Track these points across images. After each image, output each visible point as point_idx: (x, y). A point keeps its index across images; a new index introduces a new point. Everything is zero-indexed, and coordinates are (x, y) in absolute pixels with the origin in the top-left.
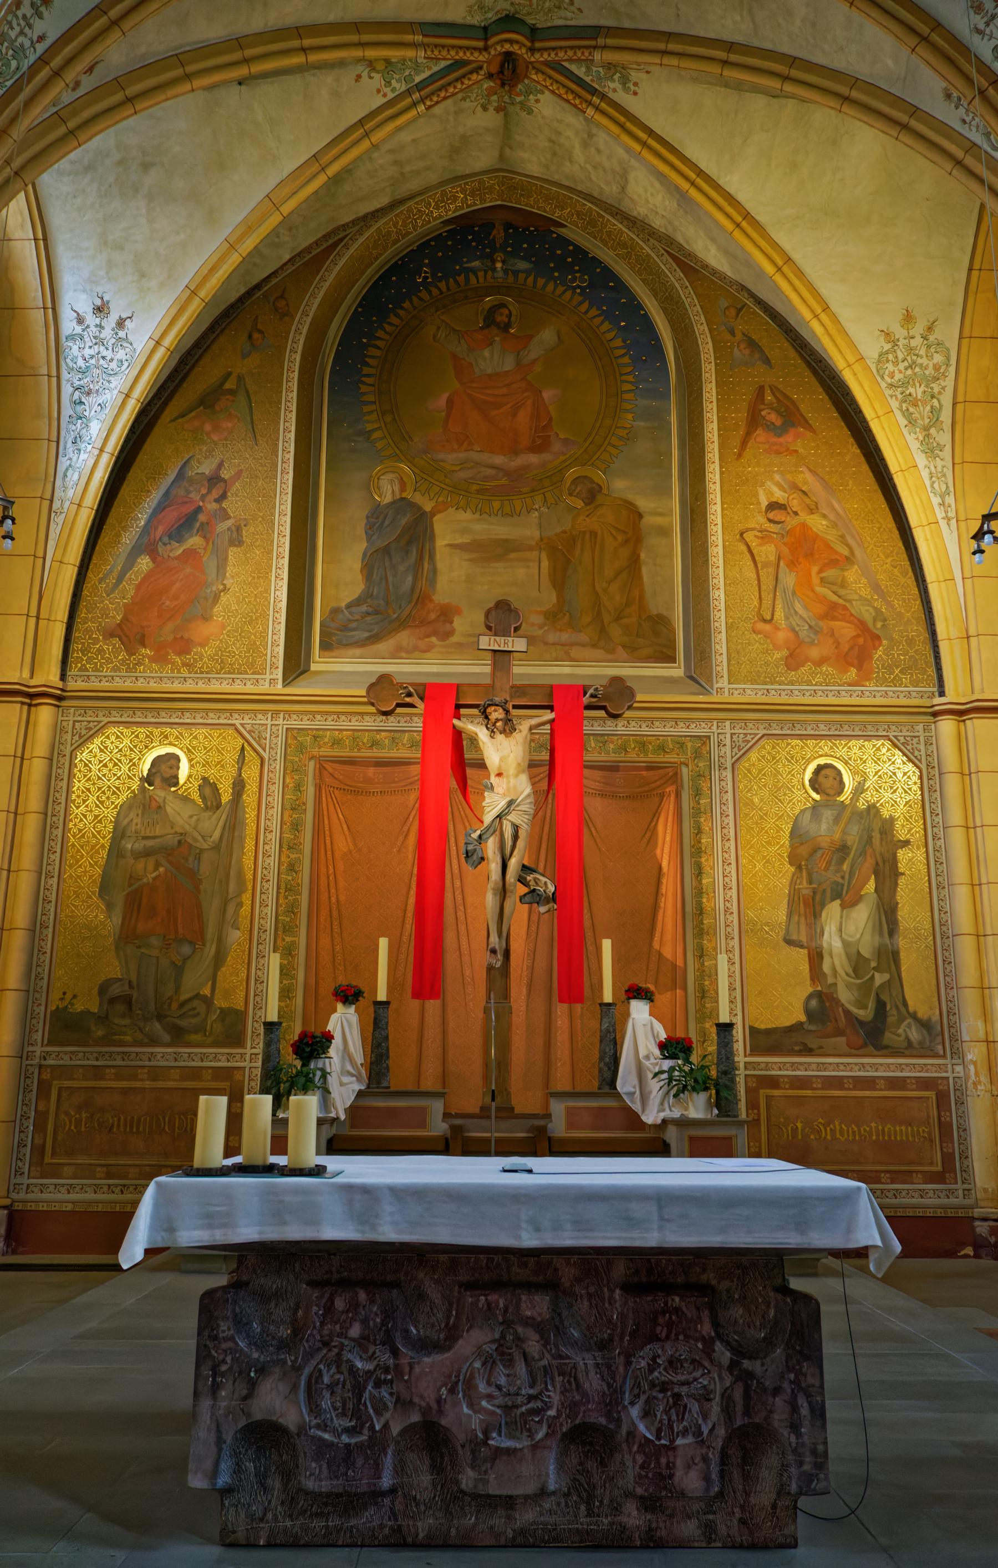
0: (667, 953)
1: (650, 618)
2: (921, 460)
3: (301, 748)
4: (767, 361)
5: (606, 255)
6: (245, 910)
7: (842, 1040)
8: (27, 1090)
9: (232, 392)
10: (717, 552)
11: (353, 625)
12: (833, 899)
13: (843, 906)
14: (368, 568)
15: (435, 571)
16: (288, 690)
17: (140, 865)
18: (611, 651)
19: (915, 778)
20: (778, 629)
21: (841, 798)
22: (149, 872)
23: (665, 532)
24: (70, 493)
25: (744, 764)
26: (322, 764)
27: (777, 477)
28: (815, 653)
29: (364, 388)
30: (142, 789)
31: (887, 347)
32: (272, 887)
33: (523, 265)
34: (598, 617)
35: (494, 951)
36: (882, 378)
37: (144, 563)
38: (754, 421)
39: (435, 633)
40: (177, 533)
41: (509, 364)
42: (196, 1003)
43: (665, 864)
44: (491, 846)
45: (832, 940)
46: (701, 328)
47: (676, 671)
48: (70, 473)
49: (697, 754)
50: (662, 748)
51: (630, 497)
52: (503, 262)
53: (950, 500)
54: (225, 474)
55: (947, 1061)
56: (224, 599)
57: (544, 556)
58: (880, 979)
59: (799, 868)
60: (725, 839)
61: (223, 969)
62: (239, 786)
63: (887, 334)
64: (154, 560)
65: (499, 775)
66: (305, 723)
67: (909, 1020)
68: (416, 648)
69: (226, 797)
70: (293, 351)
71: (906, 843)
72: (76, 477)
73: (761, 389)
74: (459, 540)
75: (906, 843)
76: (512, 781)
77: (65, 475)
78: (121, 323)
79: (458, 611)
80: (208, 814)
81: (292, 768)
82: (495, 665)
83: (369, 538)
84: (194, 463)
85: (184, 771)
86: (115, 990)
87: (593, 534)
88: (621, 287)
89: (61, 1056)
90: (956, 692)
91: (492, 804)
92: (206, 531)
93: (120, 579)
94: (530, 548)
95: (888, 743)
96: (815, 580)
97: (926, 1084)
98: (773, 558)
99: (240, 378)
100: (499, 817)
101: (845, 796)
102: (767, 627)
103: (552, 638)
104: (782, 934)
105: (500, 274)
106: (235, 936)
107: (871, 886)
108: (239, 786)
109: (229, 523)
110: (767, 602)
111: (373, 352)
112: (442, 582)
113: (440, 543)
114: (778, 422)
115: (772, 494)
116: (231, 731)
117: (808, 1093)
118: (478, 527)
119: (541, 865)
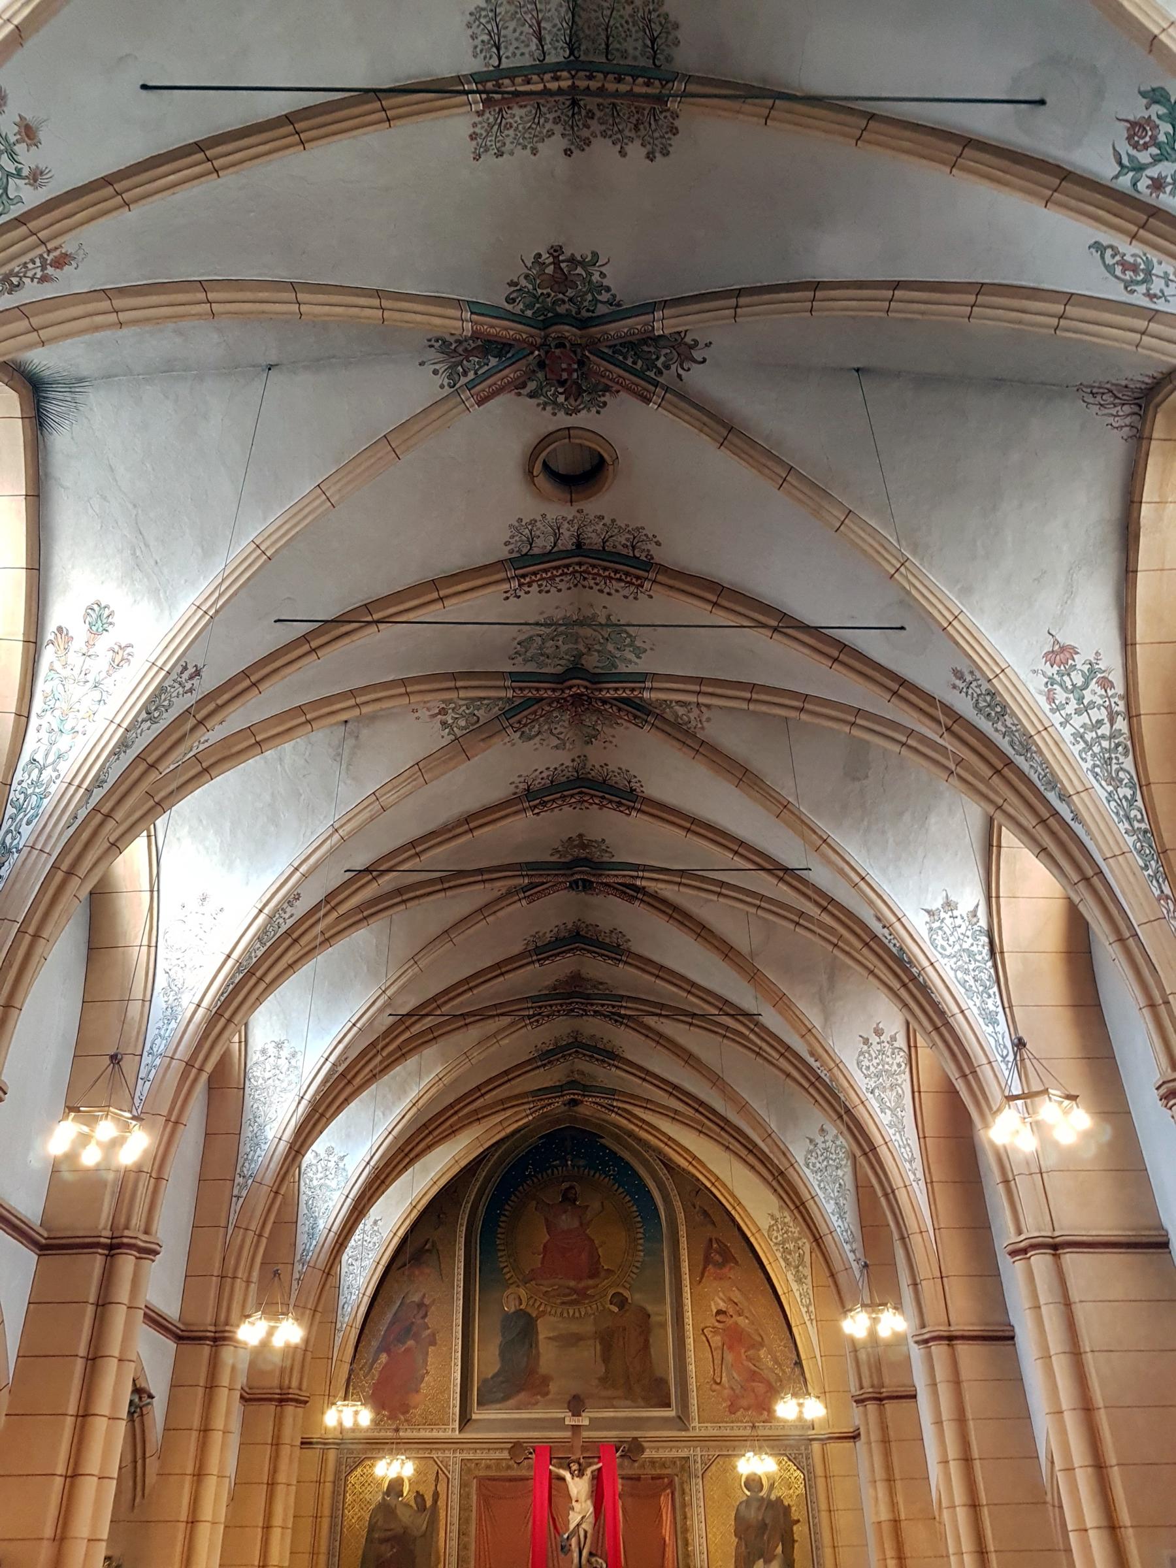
1: (656, 1380)
2: (794, 1286)
3: (469, 1470)
4: (714, 1224)
5: (627, 1156)
10: (690, 1341)
12: (759, 1558)
14: (502, 1354)
15: (538, 1354)
16: (462, 1435)
17: (383, 1547)
19: (801, 1480)
21: (761, 1494)
22: (388, 1551)
23: (663, 1325)
25: (709, 1474)
26: (482, 1481)
27: (721, 1294)
28: (744, 1403)
30: (383, 1499)
31: (773, 1222)
32: (454, 1559)
33: (582, 1162)
37: (384, 1358)
38: (707, 1260)
40: (401, 1340)
41: (576, 1224)
43: (667, 1538)
44: (574, 1541)
46: (678, 1204)
47: (671, 1413)
48: (346, 1306)
49: (683, 1468)
50: (663, 1465)
52: (572, 1161)
53: (812, 1308)
54: (427, 1301)
56: (426, 1379)
57: (598, 1344)
59: (740, 1538)
62: (436, 1496)
63: (772, 1216)
64: (389, 1355)
65: (577, 1501)
66: (471, 1456)
69: (429, 1503)
72: (349, 1309)
73: (711, 1240)
74: (551, 1335)
76: (584, 1505)
78: (375, 1222)
81: (464, 1485)
82: (573, 1434)
83: (503, 1335)
88: (636, 1174)
91: (574, 1519)
92: (416, 1337)
93: (371, 1368)
95: (785, 1458)
98: (720, 1344)
100: (578, 1525)
101: (763, 1493)
102: (718, 1387)
105: (570, 1168)
107: (780, 1548)
108: (436, 1496)
109: (429, 1331)
112: (543, 1361)
113: (541, 1337)
114: (720, 1260)
115: (718, 1304)
116: (431, 1461)
119: (599, 1552)
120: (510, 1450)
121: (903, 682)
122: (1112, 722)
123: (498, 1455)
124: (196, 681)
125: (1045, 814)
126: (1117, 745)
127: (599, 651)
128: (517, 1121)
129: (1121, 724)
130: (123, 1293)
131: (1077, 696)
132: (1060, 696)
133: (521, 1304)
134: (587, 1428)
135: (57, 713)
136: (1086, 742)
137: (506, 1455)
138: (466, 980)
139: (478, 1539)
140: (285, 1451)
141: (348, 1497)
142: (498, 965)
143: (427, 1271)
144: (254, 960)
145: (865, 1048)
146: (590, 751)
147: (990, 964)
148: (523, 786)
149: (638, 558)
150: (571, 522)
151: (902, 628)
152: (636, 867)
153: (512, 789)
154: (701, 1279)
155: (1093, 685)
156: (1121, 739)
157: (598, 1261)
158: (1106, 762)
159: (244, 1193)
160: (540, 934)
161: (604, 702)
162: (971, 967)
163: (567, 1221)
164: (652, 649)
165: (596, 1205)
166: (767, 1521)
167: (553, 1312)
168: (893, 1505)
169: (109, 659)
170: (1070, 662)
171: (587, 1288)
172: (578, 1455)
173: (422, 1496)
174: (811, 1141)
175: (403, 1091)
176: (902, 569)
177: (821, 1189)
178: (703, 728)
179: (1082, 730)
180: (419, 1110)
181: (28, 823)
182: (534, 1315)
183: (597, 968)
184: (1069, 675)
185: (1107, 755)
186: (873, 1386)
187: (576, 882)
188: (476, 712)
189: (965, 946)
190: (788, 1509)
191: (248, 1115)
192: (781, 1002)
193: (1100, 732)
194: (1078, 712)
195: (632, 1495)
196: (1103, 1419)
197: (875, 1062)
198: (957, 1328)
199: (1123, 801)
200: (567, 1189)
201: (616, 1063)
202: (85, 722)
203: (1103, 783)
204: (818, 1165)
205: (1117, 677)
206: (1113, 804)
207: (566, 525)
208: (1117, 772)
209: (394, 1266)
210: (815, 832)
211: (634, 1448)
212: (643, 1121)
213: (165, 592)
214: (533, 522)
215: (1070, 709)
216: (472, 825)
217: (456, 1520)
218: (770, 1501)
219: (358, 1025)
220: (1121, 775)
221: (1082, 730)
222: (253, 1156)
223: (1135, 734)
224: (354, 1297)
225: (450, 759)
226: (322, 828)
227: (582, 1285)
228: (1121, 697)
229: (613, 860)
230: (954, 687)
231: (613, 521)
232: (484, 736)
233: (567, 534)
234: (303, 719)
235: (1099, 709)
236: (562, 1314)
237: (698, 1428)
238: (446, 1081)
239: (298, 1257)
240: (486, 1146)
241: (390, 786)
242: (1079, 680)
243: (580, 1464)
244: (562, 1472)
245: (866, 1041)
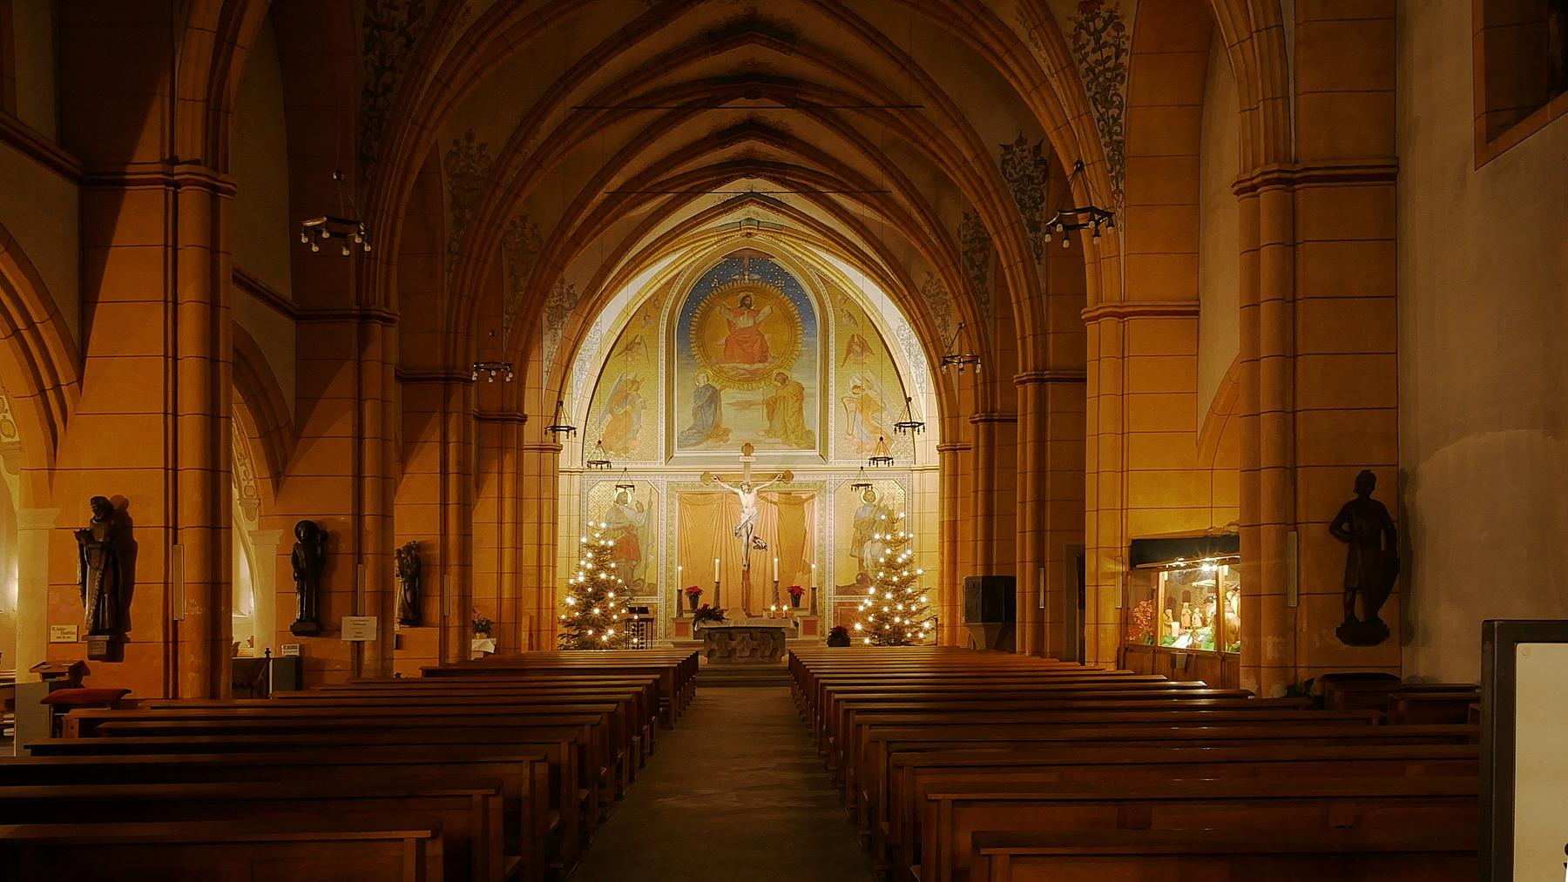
9: (637, 343)
10: (832, 407)
14: (695, 414)
16: (666, 467)
23: (813, 395)
28: (868, 447)
33: (756, 277)
38: (849, 350)
41: (751, 323)
45: (867, 555)
46: (830, 309)
49: (821, 486)
53: (924, 385)
60: (830, 519)
62: (650, 504)
70: (663, 324)
79: (731, 431)
81: (669, 496)
87: (784, 397)
88: (798, 286)
91: (744, 518)
94: (759, 404)
96: (870, 417)
98: (854, 409)
108: (650, 504)
109: (641, 400)
114: (860, 350)
123: (692, 479)
134: (754, 463)
136: (1094, 74)
139: (680, 527)
145: (966, 221)
154: (844, 363)
162: (1029, 188)
163: (744, 322)
172: (748, 480)
177: (932, 309)
182: (718, 388)
184: (1094, 21)
186: (950, 442)
189: (1028, 172)
193: (1106, 66)
194: (1094, 52)
197: (971, 232)
200: (744, 298)
208: (1113, 95)
211: (787, 476)
215: (1088, 49)
227: (756, 366)
230: (1017, 19)
235: (1110, 48)
242: (1099, 24)
244: (736, 490)
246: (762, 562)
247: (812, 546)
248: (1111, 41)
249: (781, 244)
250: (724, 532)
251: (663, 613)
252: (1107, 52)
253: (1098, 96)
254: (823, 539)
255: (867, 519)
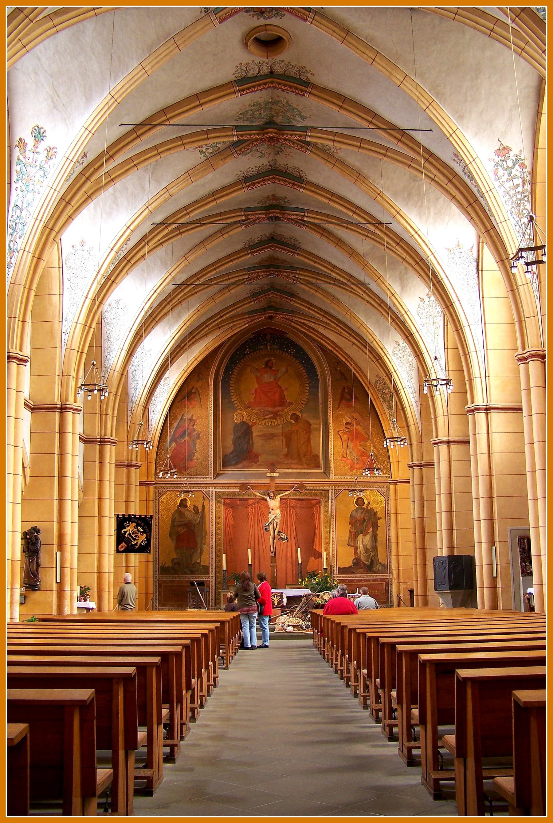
0: (317, 549)
1: (313, 456)
2: (387, 411)
3: (219, 497)
4: (346, 379)
6: (207, 540)
7: (362, 570)
8: (156, 586)
9: (194, 393)
11: (231, 460)
13: (363, 536)
14: (234, 443)
15: (253, 443)
17: (179, 529)
18: (302, 465)
19: (384, 501)
20: (348, 459)
22: (182, 530)
23: (318, 430)
24: (153, 427)
27: (348, 415)
28: (357, 466)
29: (231, 388)
30: (178, 508)
31: (377, 379)
32: (214, 534)
33: (276, 347)
34: (299, 456)
35: (272, 552)
36: (376, 388)
37: (174, 444)
38: (342, 398)
39: (253, 462)
40: (183, 435)
42: (196, 564)
44: (271, 527)
45: (360, 545)
47: (321, 470)
48: (153, 420)
49: (325, 495)
50: (316, 494)
51: (308, 419)
52: (270, 346)
54: (194, 418)
55: (389, 574)
56: (196, 455)
57: (283, 438)
58: (372, 554)
59: (352, 525)
61: (203, 555)
62: (203, 507)
65: (272, 510)
66: (220, 489)
67: (379, 564)
68: (248, 466)
69: (200, 510)
71: (380, 518)
74: (260, 434)
75: (380, 518)
77: (151, 421)
79: (260, 455)
80: (196, 515)
83: (234, 434)
84: (185, 415)
85: (189, 503)
86: (176, 561)
87: (297, 431)
88: (305, 354)
89: (165, 577)
90: (395, 476)
91: (271, 517)
92: (190, 435)
95: (376, 491)
96: (358, 445)
97: (382, 580)
98: (347, 439)
99: (196, 388)
103: (286, 462)
104: (347, 543)
106: (205, 547)
109: (196, 432)
110: (345, 451)
111: (233, 376)
112: (255, 446)
113: (254, 435)
117: (353, 583)
118: (265, 430)
120: (240, 487)
121: (431, 154)
122: (524, 185)
123: (233, 489)
124: (84, 159)
125: (489, 227)
126: (525, 197)
127: (282, 116)
128: (240, 327)
129: (528, 186)
130: (69, 428)
131: (508, 172)
132: (501, 172)
133: (243, 419)
135: (24, 181)
136: (509, 196)
137: (237, 489)
138: (212, 264)
140: (133, 488)
141: (161, 508)
142: (229, 256)
143: (194, 403)
144: (110, 272)
146: (277, 157)
147: (476, 275)
148: (242, 175)
149: (302, 80)
150: (267, 63)
151: (431, 130)
152: (303, 211)
153: (237, 177)
155: (517, 167)
156: (527, 194)
157: (284, 398)
158: (518, 205)
159: (107, 375)
160: (252, 239)
161: (285, 140)
163: (267, 378)
164: (310, 118)
165: (283, 370)
166: (366, 518)
167: (260, 423)
168: (422, 511)
169: (45, 155)
170: (507, 155)
171: (278, 411)
172: (273, 490)
173: (197, 508)
174: (396, 342)
175: (179, 316)
176: (430, 107)
178: (337, 153)
179: (508, 190)
180: (188, 326)
181: (20, 238)
182: (250, 424)
183: (283, 255)
184: (506, 161)
185: (519, 202)
186: (418, 461)
187: (271, 218)
188: (218, 145)
190: (375, 514)
191: (105, 337)
192: (379, 279)
194: (508, 181)
195: (300, 507)
196: (494, 478)
197: (426, 310)
198: (452, 438)
199: (523, 225)
201: (294, 299)
202: (38, 187)
203: (515, 217)
204: (399, 355)
205: (528, 163)
206: (517, 227)
207: (264, 64)
209: (176, 401)
210: (393, 208)
211: (302, 486)
212: (310, 327)
213: (69, 120)
214: (248, 64)
215: (504, 179)
216: (216, 197)
217: (214, 517)
218: (367, 510)
219: (158, 291)
220: (525, 211)
221: (508, 190)
222: (109, 358)
223: (533, 192)
224: (156, 416)
225: (204, 170)
226: (140, 206)
228: (529, 173)
229: (291, 206)
230: (454, 160)
231: (289, 63)
232: (222, 157)
233: (265, 68)
234: (132, 164)
236: (265, 424)
237: (333, 477)
238: (202, 311)
239: (130, 400)
240: (223, 340)
241: (174, 184)
242: (510, 163)
243: (274, 494)
244: (265, 497)
245: (422, 300)
246: (284, 550)
247: (320, 538)
248: (519, 175)
249: (293, 324)
250: (256, 528)
251: (214, 587)
252: (516, 181)
253: (513, 210)
254: (328, 533)
255: (359, 519)
